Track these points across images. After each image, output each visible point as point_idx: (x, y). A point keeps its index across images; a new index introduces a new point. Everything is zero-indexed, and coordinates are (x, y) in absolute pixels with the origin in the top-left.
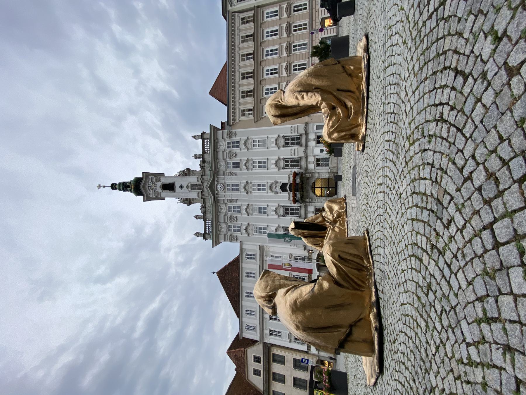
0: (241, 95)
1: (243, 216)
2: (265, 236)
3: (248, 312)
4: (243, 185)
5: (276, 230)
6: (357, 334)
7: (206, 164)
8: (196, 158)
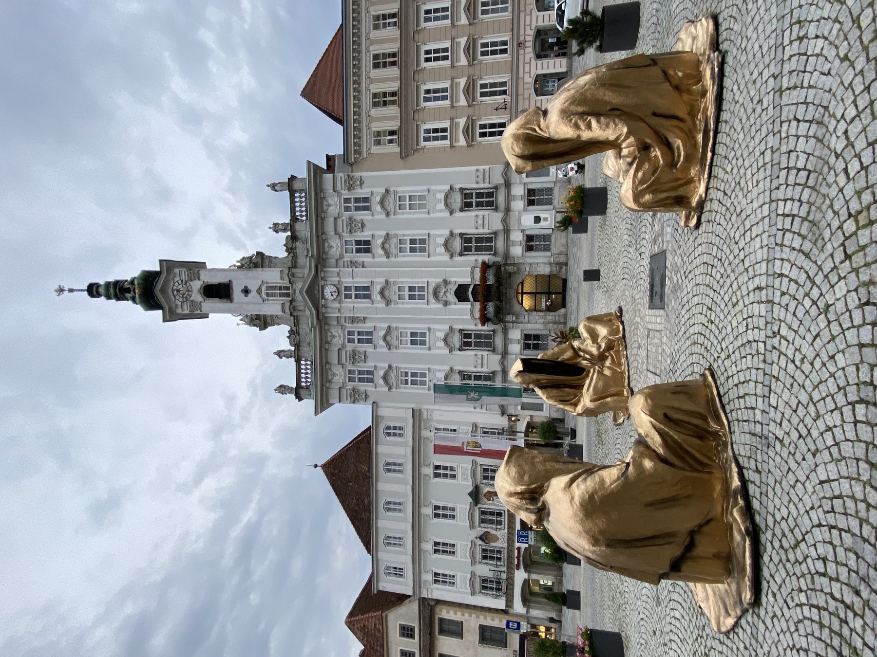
1: (378, 350)
4: (378, 288)
5: (446, 378)
6: (704, 547)
8: (277, 232)
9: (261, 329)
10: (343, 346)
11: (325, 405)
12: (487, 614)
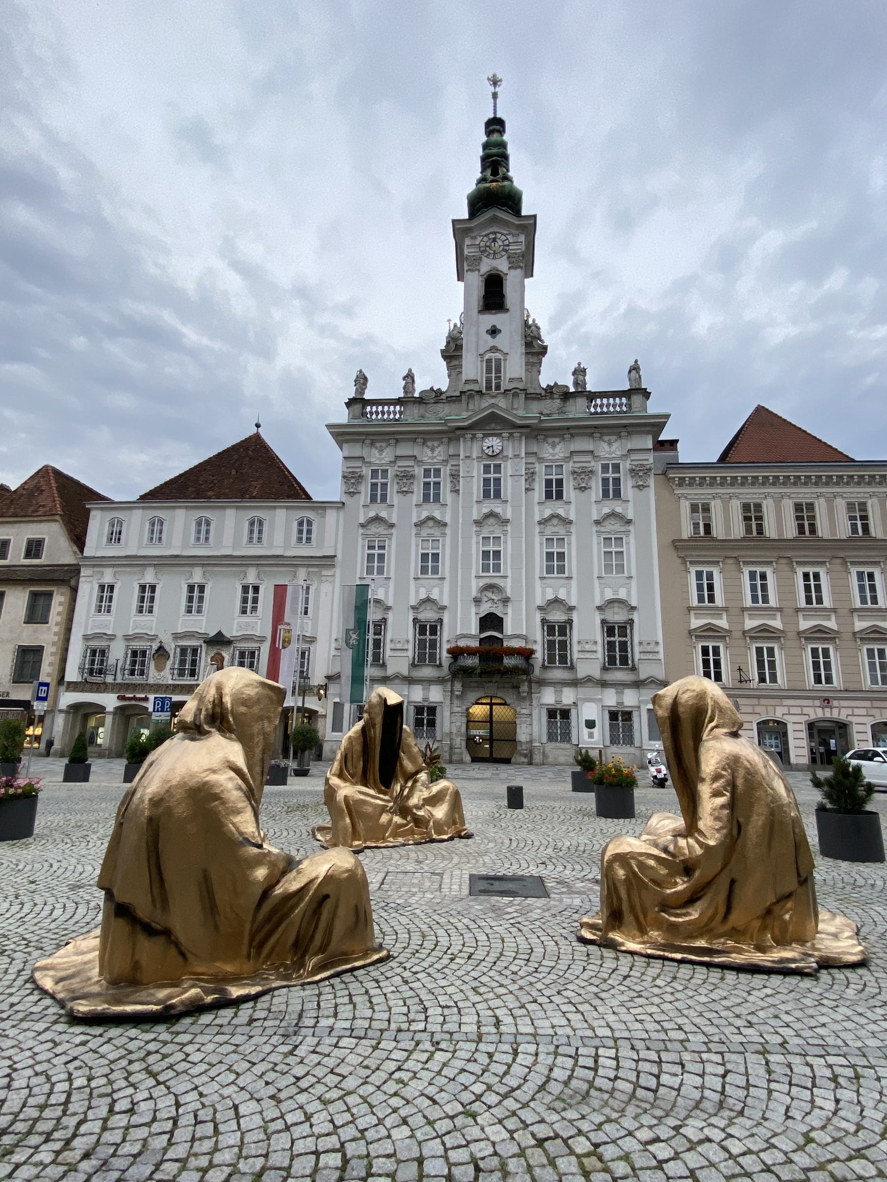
0: (752, 502)
1: (415, 510)
2: (358, 572)
3: (157, 526)
4: (498, 510)
5: (377, 601)
6: (149, 950)
7: (558, 402)
8: (574, 373)
9: (442, 351)
10: (420, 463)
11: (340, 438)
12: (58, 657)
